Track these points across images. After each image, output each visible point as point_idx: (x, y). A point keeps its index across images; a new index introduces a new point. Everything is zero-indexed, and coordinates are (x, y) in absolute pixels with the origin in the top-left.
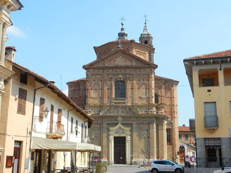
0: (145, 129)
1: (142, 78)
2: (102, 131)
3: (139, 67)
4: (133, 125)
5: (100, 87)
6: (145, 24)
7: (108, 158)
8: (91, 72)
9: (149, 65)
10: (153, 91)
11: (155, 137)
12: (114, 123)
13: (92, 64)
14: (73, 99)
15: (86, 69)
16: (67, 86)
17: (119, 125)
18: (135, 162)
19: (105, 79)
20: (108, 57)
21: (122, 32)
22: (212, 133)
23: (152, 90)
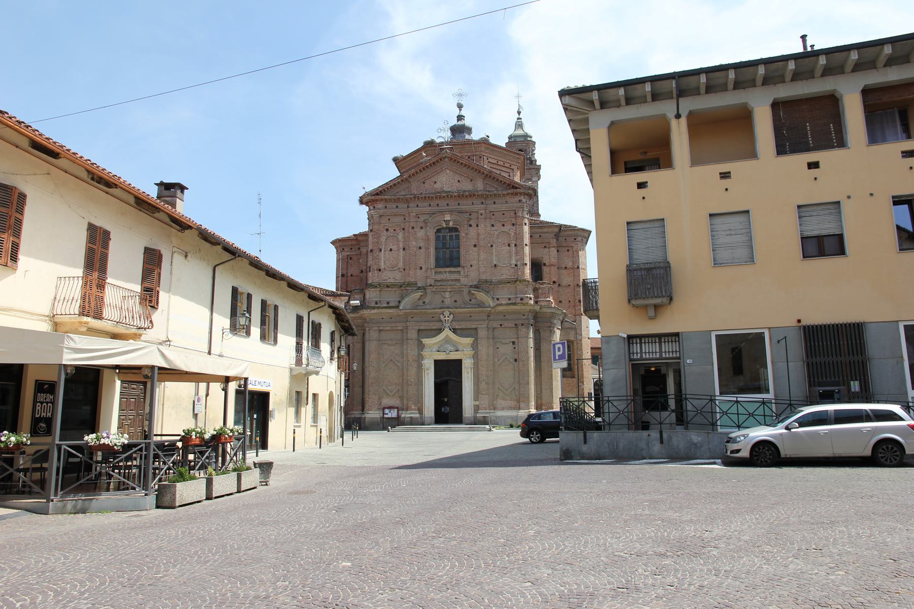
0: (508, 341)
1: (500, 220)
2: (405, 347)
3: (491, 195)
4: (479, 331)
5: (401, 243)
6: (519, 113)
7: (420, 411)
8: (378, 211)
9: (516, 188)
10: (527, 250)
11: (532, 359)
12: (434, 328)
13: (381, 192)
14: (347, 277)
15: (367, 204)
16: (333, 247)
17: (447, 332)
19: (412, 224)
20: (417, 172)
21: (460, 123)
22: (651, 318)
23: (523, 248)
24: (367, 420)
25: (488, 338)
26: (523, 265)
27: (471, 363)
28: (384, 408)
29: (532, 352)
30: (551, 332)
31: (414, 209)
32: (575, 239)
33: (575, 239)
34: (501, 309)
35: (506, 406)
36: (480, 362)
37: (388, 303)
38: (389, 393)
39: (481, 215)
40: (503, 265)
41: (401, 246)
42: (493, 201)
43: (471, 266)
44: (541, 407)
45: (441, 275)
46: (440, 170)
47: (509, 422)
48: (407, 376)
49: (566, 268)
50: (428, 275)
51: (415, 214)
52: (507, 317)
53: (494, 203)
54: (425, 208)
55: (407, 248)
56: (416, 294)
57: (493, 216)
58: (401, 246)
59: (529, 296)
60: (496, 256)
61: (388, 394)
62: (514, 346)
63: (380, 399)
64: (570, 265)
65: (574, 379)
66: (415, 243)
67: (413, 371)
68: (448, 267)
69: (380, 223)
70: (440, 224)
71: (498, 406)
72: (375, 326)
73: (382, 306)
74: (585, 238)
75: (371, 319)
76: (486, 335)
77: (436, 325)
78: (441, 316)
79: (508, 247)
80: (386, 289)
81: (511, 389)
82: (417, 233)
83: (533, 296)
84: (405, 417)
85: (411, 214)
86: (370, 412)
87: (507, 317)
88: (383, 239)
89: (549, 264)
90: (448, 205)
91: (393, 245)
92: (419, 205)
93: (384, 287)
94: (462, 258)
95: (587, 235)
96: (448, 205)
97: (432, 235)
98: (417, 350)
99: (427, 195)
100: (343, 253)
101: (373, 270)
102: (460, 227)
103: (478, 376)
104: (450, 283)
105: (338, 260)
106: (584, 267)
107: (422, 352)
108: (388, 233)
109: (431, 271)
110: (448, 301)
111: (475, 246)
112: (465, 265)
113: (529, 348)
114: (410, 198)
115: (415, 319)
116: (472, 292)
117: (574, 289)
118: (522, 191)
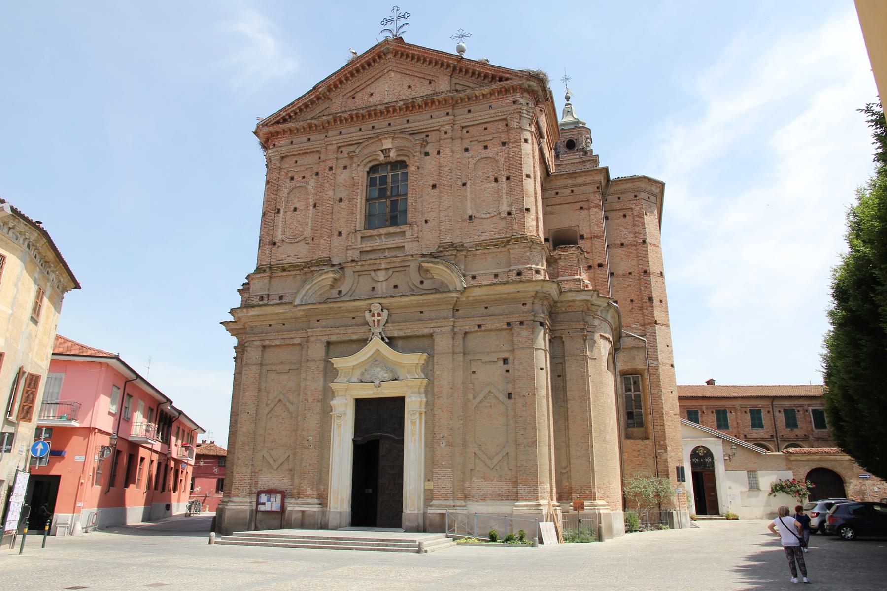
0: (494, 357)
2: (303, 376)
3: (462, 99)
4: (437, 339)
5: (311, 197)
6: (568, 98)
7: (323, 499)
8: (279, 149)
9: (507, 79)
12: (355, 337)
17: (376, 345)
18: (443, 515)
25: (454, 353)
26: (522, 211)
27: (421, 402)
32: (636, 196)
33: (636, 196)
34: (478, 294)
35: (490, 492)
36: (436, 401)
37: (281, 298)
38: (272, 462)
39: (446, 133)
40: (484, 216)
41: (311, 200)
42: (467, 109)
43: (426, 221)
44: (570, 495)
49: (622, 245)
50: (350, 244)
51: (335, 147)
54: (352, 135)
56: (323, 277)
58: (311, 200)
59: (534, 266)
60: (472, 199)
61: (271, 467)
63: (255, 473)
64: (630, 238)
65: (647, 442)
66: (333, 192)
67: (313, 421)
69: (281, 169)
70: (374, 157)
71: (474, 492)
72: (257, 338)
73: (271, 303)
75: (252, 327)
76: (451, 347)
77: (356, 333)
78: (367, 314)
79: (494, 184)
80: (280, 274)
81: (499, 457)
82: (338, 177)
85: (329, 147)
87: (492, 310)
88: (284, 193)
89: (589, 236)
90: (389, 124)
91: (299, 201)
92: (343, 132)
94: (410, 209)
96: (389, 124)
97: (360, 175)
98: (322, 380)
104: (386, 255)
106: (654, 242)
108: (293, 183)
111: (434, 186)
112: (413, 220)
113: (537, 371)
114: (329, 122)
115: (323, 323)
116: (424, 265)
117: (640, 279)
118: (516, 82)
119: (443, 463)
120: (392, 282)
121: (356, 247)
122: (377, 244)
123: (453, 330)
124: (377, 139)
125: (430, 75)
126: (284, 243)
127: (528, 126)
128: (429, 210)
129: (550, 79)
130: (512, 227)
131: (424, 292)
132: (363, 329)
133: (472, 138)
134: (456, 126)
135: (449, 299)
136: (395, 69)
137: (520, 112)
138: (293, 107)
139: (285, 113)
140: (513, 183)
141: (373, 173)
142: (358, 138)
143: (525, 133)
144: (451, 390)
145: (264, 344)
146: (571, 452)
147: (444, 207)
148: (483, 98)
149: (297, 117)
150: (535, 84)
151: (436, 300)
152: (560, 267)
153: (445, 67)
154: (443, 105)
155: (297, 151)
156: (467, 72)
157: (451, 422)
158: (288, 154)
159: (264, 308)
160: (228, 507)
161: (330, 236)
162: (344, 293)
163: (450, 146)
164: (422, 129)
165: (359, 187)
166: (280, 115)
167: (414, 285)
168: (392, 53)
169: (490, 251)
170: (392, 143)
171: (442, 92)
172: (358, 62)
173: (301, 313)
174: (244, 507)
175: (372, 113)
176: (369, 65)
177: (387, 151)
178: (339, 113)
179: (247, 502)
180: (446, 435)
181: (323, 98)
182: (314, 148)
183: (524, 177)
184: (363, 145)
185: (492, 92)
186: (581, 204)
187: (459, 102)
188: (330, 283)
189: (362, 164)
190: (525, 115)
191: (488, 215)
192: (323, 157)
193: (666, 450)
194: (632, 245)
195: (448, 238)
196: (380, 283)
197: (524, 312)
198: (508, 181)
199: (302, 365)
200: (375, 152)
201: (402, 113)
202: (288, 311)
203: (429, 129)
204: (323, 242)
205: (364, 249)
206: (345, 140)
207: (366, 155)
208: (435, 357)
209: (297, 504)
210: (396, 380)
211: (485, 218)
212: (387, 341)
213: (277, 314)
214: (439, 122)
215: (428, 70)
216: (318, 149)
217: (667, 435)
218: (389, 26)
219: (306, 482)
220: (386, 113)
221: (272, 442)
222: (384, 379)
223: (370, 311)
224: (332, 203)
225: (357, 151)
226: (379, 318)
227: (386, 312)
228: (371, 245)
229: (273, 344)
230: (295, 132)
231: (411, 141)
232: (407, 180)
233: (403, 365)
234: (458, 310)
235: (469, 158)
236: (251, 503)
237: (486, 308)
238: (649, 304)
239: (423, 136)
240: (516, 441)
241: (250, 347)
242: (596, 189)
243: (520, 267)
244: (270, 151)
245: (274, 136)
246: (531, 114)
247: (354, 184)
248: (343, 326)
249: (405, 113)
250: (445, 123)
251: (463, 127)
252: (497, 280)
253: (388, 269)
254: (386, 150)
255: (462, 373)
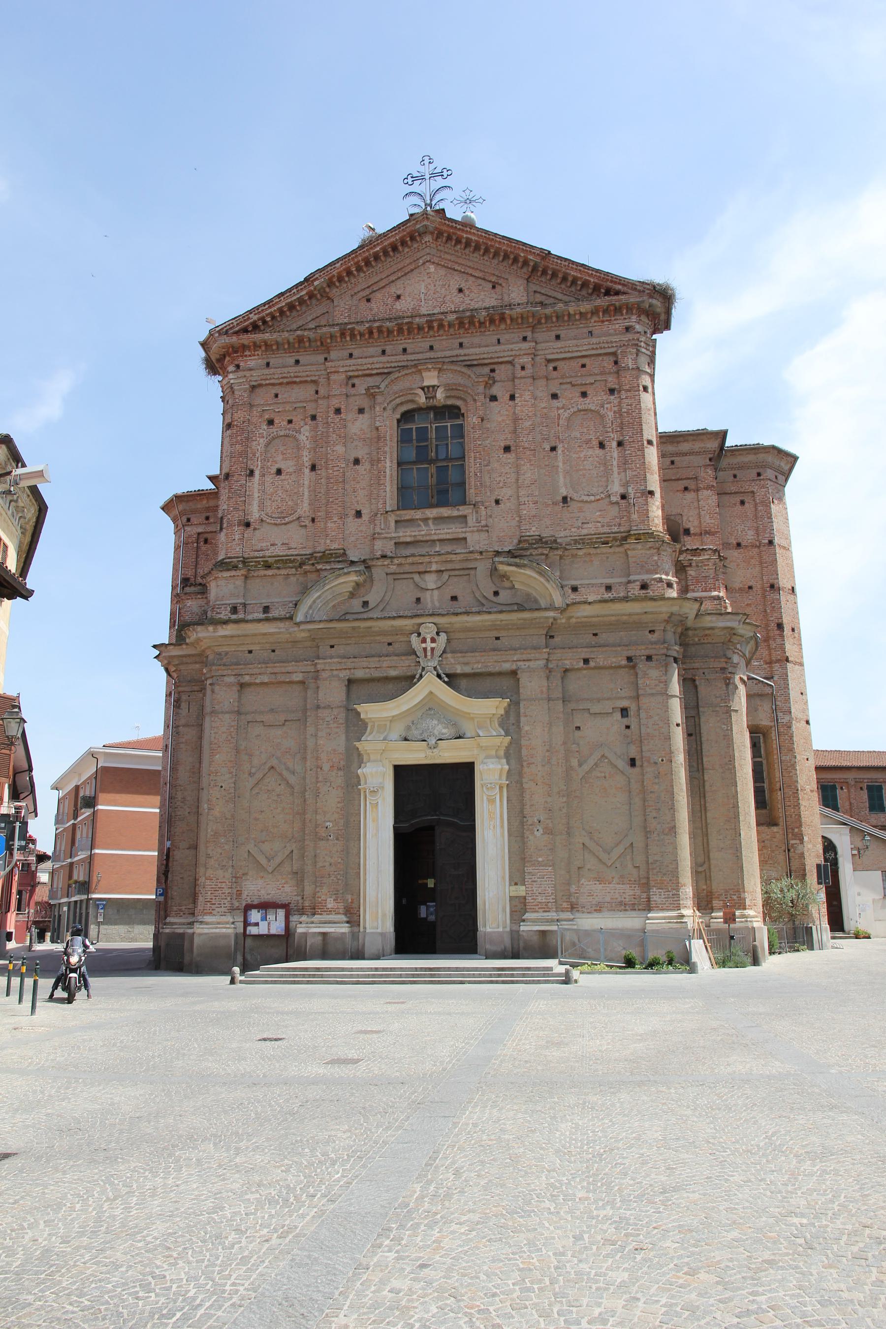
0: (607, 706)
1: (573, 380)
2: (311, 730)
3: (547, 318)
4: (524, 679)
5: (305, 453)
7: (353, 916)
8: (248, 374)
9: (617, 293)
11: (680, 758)
12: (393, 673)
18: (543, 933)
19: (335, 403)
23: (642, 449)
24: (197, 940)
25: (549, 699)
26: (643, 494)
27: (501, 770)
28: (248, 908)
29: (678, 738)
30: (727, 685)
31: (341, 363)
32: (759, 474)
33: (759, 474)
34: (585, 614)
35: (608, 899)
36: (526, 770)
37: (266, 609)
38: (264, 862)
39: (523, 368)
40: (586, 498)
42: (553, 334)
43: (497, 502)
45: (413, 529)
46: (412, 267)
47: (621, 949)
48: (316, 812)
49: (739, 545)
50: (378, 530)
51: (343, 376)
52: (603, 637)
53: (558, 337)
54: (371, 360)
55: (320, 463)
56: (341, 580)
57: (555, 373)
58: (305, 459)
61: (260, 867)
62: (625, 721)
63: (237, 879)
64: (749, 537)
65: (775, 829)
66: (344, 449)
68: (432, 506)
69: (251, 406)
70: (410, 397)
71: (583, 900)
72: (230, 672)
73: (250, 617)
74: (783, 473)
75: (220, 654)
76: (544, 689)
77: (397, 667)
78: (414, 638)
79: (598, 451)
80: (262, 573)
81: (620, 849)
82: (349, 425)
83: (675, 579)
84: (305, 935)
85: (333, 377)
86: (208, 919)
87: (603, 637)
88: (258, 445)
89: (698, 530)
90: (431, 348)
92: (356, 353)
93: (256, 566)
95: (787, 468)
96: (431, 348)
97: (388, 424)
98: (343, 737)
99: (377, 324)
100: (188, 529)
101: (230, 525)
102: (466, 406)
103: (522, 811)
104: (437, 549)
105: (177, 548)
106: (783, 543)
107: (357, 744)
108: (273, 430)
109: (386, 520)
110: (432, 602)
111: (507, 449)
112: (479, 499)
114: (332, 337)
115: (340, 650)
116: (503, 568)
117: (764, 597)
118: (633, 299)
119: (540, 859)
120: (448, 592)
121: (389, 536)
122: (423, 533)
123: (546, 666)
124: (414, 370)
125: (494, 275)
126: (264, 524)
127: (647, 366)
128: (501, 485)
129: (678, 296)
130: (629, 517)
131: (500, 608)
132: (408, 661)
133: (562, 378)
134: (538, 359)
135: (542, 620)
136: (436, 260)
137: (637, 345)
138: (270, 307)
139: (257, 316)
140: (629, 452)
141: (406, 422)
142: (381, 365)
143: (643, 376)
144: (547, 754)
145: (242, 681)
146: (711, 843)
147: (526, 483)
148: (580, 320)
149: (276, 324)
150: (659, 304)
151: (522, 621)
152: (690, 578)
153: (520, 265)
154: (518, 324)
155: (278, 378)
156: (554, 275)
157: (549, 799)
158: (264, 382)
159: (243, 626)
160: (198, 931)
161: (343, 516)
162: (371, 605)
163: (531, 388)
164: (484, 359)
165: (388, 442)
166: (249, 318)
167: (484, 596)
168: (432, 233)
169: (598, 551)
170: (438, 377)
171: (519, 304)
172: (378, 244)
173: (304, 635)
174: (224, 930)
175: (405, 328)
176: (395, 248)
177: (431, 389)
178: (350, 323)
179: (227, 923)
180: (542, 819)
181: (319, 296)
182: (307, 376)
183: (645, 443)
184: (393, 376)
185: (594, 311)
186: (685, 483)
187: (543, 321)
188: (351, 589)
189: (390, 407)
190: (643, 350)
191: (592, 498)
192: (322, 392)
193: (802, 841)
194: (753, 546)
195: (534, 529)
196: (429, 593)
197: (652, 643)
198: (620, 448)
199: (308, 714)
200: (411, 389)
201: (452, 330)
202: (282, 630)
203: (496, 360)
204: (333, 525)
205: (402, 540)
206: (359, 368)
207: (396, 393)
208: (521, 705)
209: (312, 923)
210: (460, 737)
211: (587, 502)
212: (446, 679)
213: (265, 634)
214: (512, 350)
215: (492, 266)
216: (314, 378)
217: (803, 820)
218: (416, 187)
219: (325, 890)
220: (426, 330)
221: (262, 831)
222: (442, 737)
223: (419, 634)
224: (343, 466)
225: (383, 386)
226: (433, 645)
227: (443, 637)
228: (413, 534)
229: (258, 681)
230: (274, 347)
231: (469, 376)
232: (462, 437)
233: (472, 716)
234: (552, 637)
235: (558, 408)
236: (233, 923)
237: (595, 635)
238: (778, 632)
239: (486, 370)
240: (645, 828)
241: (219, 685)
242: (708, 462)
243: (645, 577)
244: (231, 376)
245: (236, 352)
246: (651, 349)
247: (379, 438)
248: (373, 656)
249: (457, 332)
250: (522, 352)
251: (549, 361)
252: (610, 595)
253: (440, 571)
254: (428, 387)
255: (562, 728)
